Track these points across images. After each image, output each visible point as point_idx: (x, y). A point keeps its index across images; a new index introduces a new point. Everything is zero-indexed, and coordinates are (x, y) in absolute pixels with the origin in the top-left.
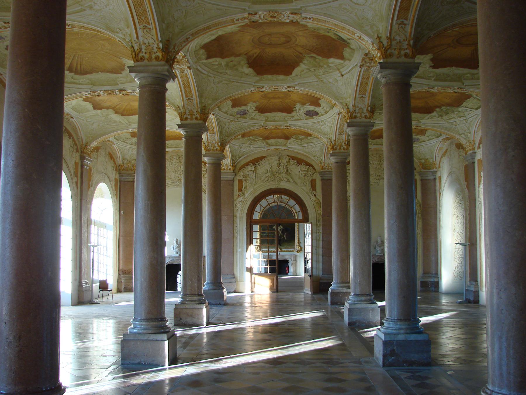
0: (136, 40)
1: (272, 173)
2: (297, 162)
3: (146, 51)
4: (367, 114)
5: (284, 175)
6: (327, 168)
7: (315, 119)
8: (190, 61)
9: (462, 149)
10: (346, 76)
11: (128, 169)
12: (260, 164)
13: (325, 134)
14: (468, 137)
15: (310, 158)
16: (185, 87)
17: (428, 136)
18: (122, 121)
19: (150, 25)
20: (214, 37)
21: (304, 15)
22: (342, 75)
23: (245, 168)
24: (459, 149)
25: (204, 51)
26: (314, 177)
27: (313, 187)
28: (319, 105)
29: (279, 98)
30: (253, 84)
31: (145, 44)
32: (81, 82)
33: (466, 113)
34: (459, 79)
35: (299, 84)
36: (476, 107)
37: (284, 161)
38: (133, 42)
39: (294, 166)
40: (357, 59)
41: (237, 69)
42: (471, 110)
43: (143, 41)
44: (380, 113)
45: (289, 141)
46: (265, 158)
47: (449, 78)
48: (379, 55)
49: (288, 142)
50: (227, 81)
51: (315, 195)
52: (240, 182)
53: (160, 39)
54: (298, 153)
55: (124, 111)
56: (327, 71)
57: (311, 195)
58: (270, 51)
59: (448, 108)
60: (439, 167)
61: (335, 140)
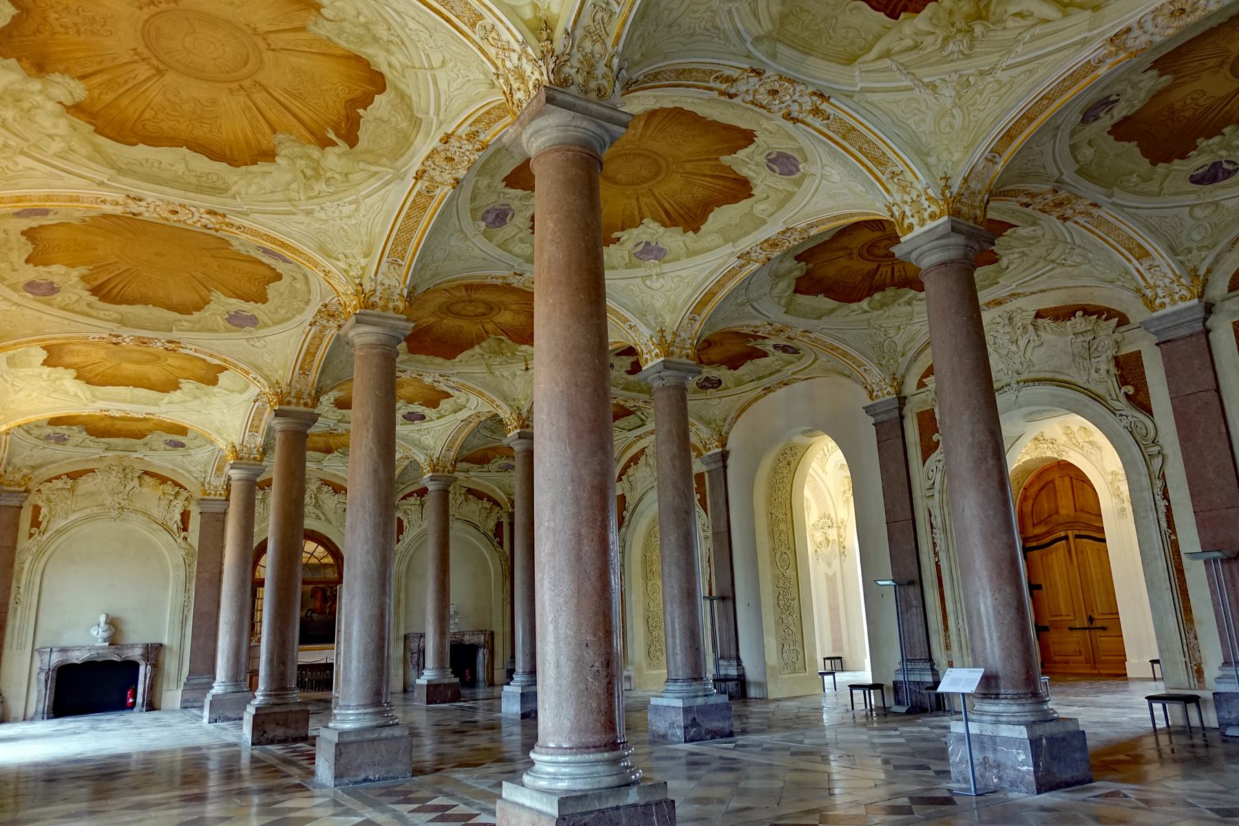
18: (79, 393)
32: (101, 315)
45: (329, 456)
53: (408, 283)
54: (335, 475)
61: (438, 459)
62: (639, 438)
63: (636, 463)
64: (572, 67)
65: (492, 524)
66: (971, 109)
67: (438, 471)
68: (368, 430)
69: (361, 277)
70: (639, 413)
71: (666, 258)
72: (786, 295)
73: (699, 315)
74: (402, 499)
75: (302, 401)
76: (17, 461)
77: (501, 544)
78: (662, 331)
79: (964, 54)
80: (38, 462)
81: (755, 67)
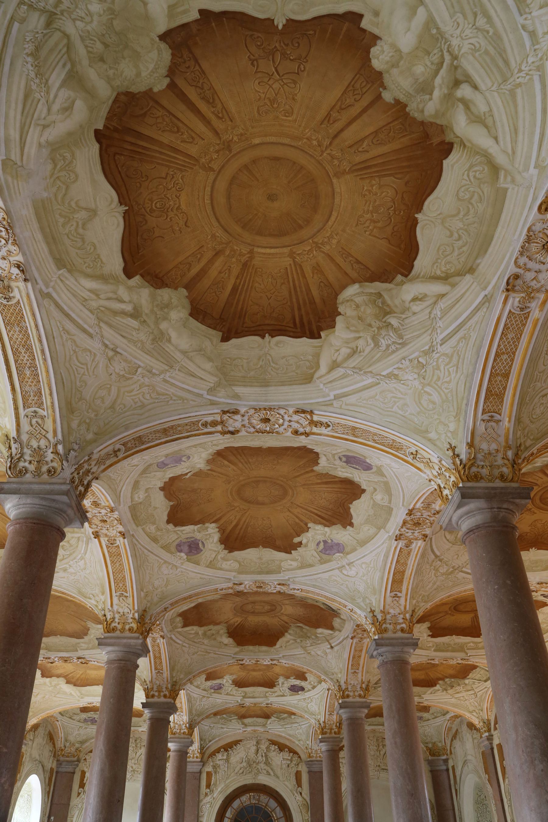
0: (110, 608)
1: (248, 763)
2: (279, 748)
3: (119, 621)
4: (362, 693)
5: (262, 765)
6: (315, 755)
7: (301, 696)
8: (165, 629)
10: (336, 649)
11: (70, 755)
12: (234, 751)
13: (312, 714)
15: (294, 742)
17: (433, 714)
18: (73, 693)
19: (127, 593)
20: (193, 605)
21: (291, 587)
22: (332, 647)
23: (215, 755)
24: (472, 730)
25: (180, 618)
27: (299, 783)
28: (305, 679)
29: (259, 670)
30: (232, 655)
31: (119, 613)
33: (474, 686)
34: (461, 648)
35: (283, 656)
36: (485, 679)
37: (263, 747)
38: (107, 611)
39: (275, 753)
40: (348, 629)
41: (215, 639)
43: (117, 610)
44: (375, 687)
45: (269, 721)
46: (240, 743)
47: (450, 648)
48: (373, 630)
49: (269, 722)
51: (301, 794)
52: (209, 774)
53: (136, 608)
54: (280, 736)
55: (78, 680)
57: (296, 794)
58: (253, 620)
59: (453, 680)
60: (451, 753)
61: (324, 722)
64: (25, 461)
66: (439, 383)
67: (326, 733)
73: (401, 592)
75: (162, 694)
76: (71, 738)
79: (400, 344)
80: (84, 738)
81: (226, 409)
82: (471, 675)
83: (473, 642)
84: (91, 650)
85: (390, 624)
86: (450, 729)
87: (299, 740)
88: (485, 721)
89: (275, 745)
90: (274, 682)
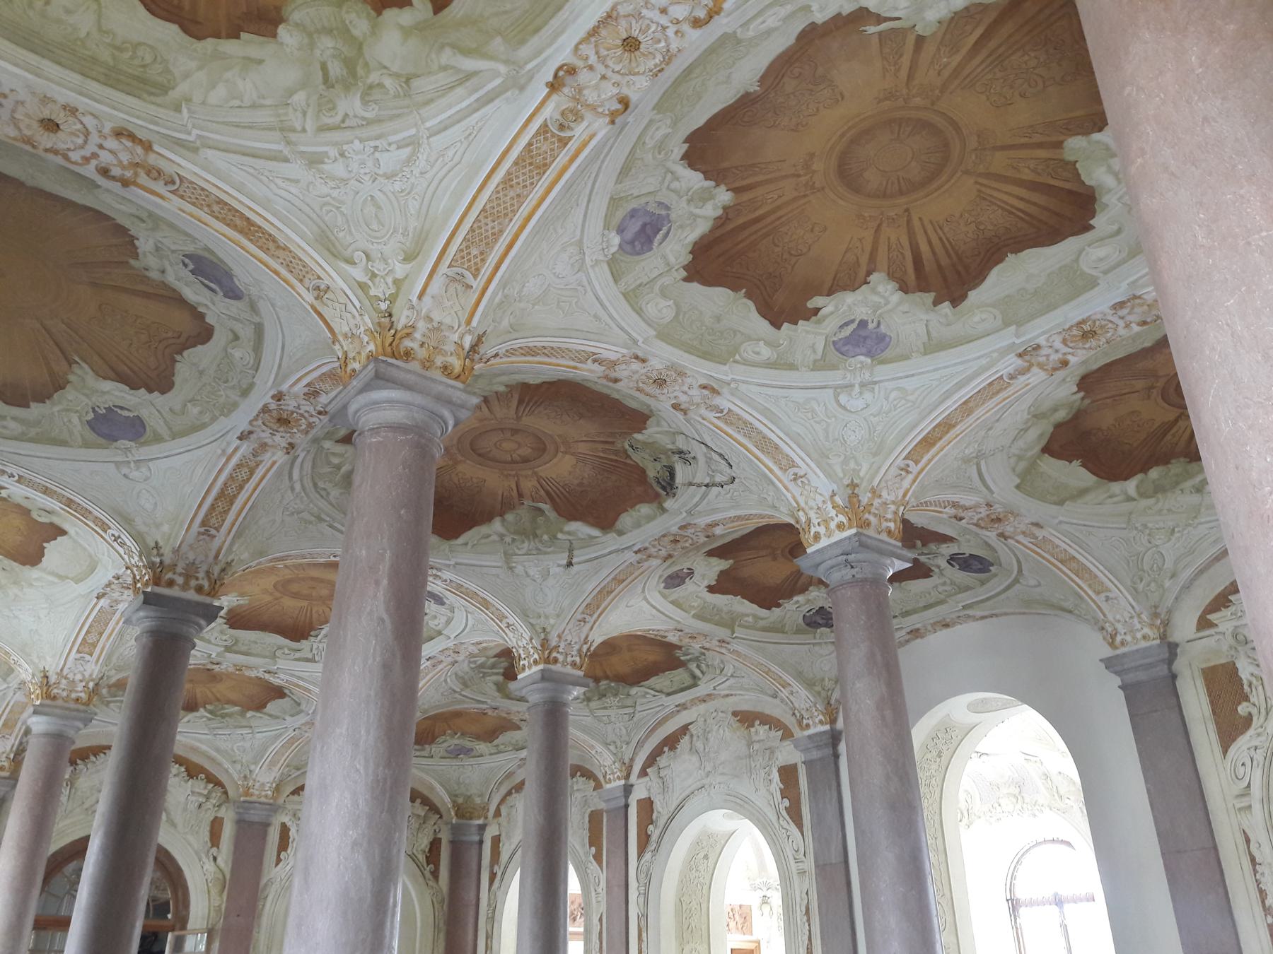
0: (415, 300)
2: (187, 770)
3: (424, 340)
4: (578, 659)
9: (582, 775)
10: (575, 568)
14: (622, 752)
15: (220, 765)
16: (222, 494)
17: (497, 746)
26: (222, 813)
31: (431, 320)
35: (457, 564)
36: (671, 690)
39: (177, 779)
42: (657, 694)
45: (191, 716)
46: (106, 751)
50: (312, 514)
51: (215, 859)
54: (195, 750)
56: (537, 549)
59: (613, 684)
60: (498, 813)
62: (683, 707)
63: (673, 748)
65: (424, 842)
68: (377, 583)
69: (392, 299)
70: (693, 666)
71: (888, 353)
72: (1029, 454)
74: (293, 793)
77: (435, 874)
78: (853, 485)
82: (653, 681)
83: (755, 616)
84: (32, 445)
85: (875, 515)
86: (510, 775)
87: (235, 762)
88: (627, 761)
89: (180, 765)
90: (312, 629)
